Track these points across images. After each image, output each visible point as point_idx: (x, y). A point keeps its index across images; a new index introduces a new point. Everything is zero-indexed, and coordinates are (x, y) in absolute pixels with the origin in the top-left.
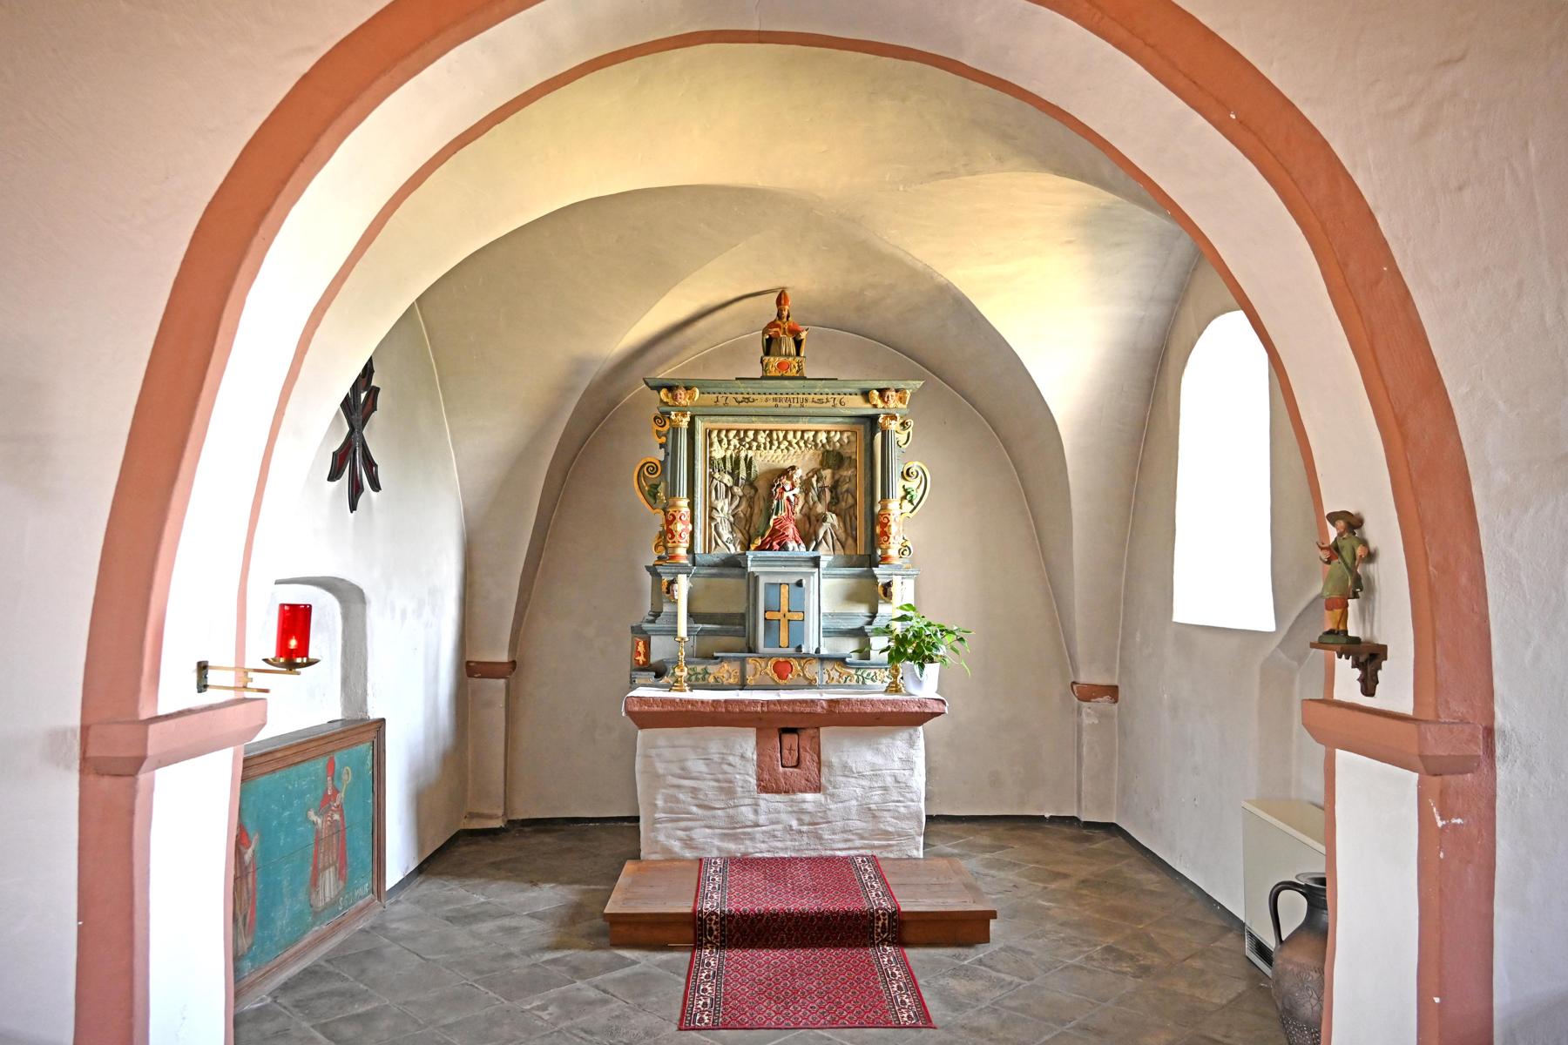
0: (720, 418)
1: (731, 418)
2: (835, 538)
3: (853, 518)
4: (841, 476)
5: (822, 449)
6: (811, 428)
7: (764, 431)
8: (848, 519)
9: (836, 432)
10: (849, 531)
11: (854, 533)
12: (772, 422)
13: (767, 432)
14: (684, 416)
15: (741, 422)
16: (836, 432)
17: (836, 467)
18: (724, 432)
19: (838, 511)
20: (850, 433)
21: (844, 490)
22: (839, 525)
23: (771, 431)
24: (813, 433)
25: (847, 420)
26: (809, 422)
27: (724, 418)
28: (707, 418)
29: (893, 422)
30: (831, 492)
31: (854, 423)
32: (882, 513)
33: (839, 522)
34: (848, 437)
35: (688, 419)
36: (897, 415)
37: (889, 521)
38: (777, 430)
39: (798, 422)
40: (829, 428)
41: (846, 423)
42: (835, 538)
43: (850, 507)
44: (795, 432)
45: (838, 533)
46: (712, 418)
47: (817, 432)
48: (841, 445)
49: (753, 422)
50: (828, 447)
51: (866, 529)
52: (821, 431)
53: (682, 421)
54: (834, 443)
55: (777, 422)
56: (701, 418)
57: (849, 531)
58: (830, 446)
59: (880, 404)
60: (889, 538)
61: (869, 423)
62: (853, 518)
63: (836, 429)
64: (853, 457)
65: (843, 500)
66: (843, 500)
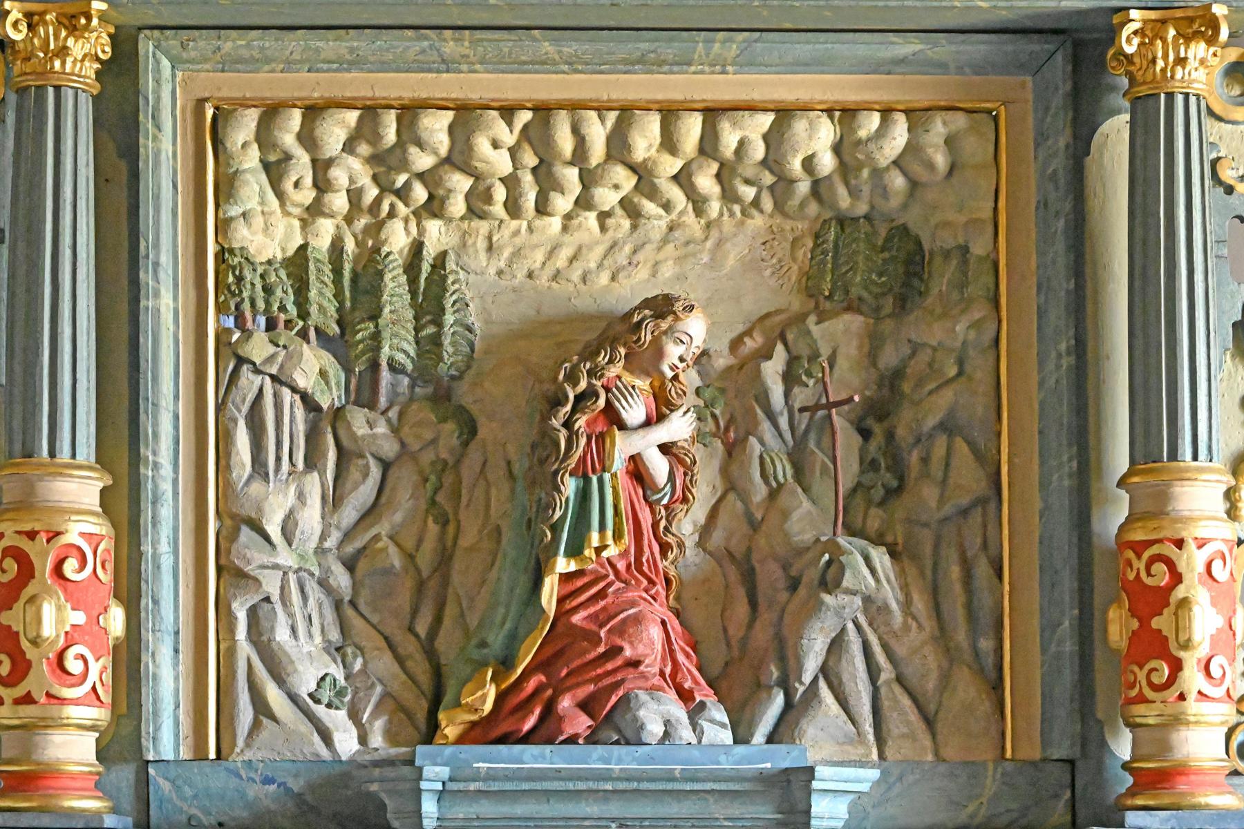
0: (269, 41)
1: (329, 45)
2: (887, 673)
3: (983, 569)
4: (916, 348)
5: (813, 208)
6: (756, 96)
7: (507, 112)
8: (955, 571)
9: (886, 112)
10: (961, 636)
11: (986, 644)
12: (543, 64)
13: (525, 117)
14: (73, 23)
15: (384, 67)
16: (886, 112)
17: (888, 304)
18: (296, 117)
19: (898, 534)
20: (960, 121)
21: (931, 422)
22: (907, 605)
23: (544, 111)
24: (767, 120)
25: (944, 48)
26: (746, 63)
27: (295, 43)
28: (203, 43)
29: (1199, 49)
30: (865, 434)
31: (979, 70)
32: (1139, 536)
33: (905, 588)
34: (950, 142)
35: (97, 42)
36: (1219, 10)
37: (1177, 578)
38: (574, 107)
39: (684, 63)
40: (851, 97)
41: (941, 67)
42: (887, 673)
43: (965, 512)
44: (670, 113)
45: (901, 650)
46: (232, 43)
47: (784, 114)
48: (914, 185)
49: (448, 65)
50: (844, 199)
51: (1050, 627)
52: (806, 108)
53: (63, 52)
54: (877, 173)
55: (574, 64)
56: (172, 40)
57: (961, 636)
58: (854, 193)
60: (1177, 666)
61: (1060, 64)
62: (983, 569)
63: (885, 97)
64: (979, 248)
65: (925, 475)
66: (925, 475)
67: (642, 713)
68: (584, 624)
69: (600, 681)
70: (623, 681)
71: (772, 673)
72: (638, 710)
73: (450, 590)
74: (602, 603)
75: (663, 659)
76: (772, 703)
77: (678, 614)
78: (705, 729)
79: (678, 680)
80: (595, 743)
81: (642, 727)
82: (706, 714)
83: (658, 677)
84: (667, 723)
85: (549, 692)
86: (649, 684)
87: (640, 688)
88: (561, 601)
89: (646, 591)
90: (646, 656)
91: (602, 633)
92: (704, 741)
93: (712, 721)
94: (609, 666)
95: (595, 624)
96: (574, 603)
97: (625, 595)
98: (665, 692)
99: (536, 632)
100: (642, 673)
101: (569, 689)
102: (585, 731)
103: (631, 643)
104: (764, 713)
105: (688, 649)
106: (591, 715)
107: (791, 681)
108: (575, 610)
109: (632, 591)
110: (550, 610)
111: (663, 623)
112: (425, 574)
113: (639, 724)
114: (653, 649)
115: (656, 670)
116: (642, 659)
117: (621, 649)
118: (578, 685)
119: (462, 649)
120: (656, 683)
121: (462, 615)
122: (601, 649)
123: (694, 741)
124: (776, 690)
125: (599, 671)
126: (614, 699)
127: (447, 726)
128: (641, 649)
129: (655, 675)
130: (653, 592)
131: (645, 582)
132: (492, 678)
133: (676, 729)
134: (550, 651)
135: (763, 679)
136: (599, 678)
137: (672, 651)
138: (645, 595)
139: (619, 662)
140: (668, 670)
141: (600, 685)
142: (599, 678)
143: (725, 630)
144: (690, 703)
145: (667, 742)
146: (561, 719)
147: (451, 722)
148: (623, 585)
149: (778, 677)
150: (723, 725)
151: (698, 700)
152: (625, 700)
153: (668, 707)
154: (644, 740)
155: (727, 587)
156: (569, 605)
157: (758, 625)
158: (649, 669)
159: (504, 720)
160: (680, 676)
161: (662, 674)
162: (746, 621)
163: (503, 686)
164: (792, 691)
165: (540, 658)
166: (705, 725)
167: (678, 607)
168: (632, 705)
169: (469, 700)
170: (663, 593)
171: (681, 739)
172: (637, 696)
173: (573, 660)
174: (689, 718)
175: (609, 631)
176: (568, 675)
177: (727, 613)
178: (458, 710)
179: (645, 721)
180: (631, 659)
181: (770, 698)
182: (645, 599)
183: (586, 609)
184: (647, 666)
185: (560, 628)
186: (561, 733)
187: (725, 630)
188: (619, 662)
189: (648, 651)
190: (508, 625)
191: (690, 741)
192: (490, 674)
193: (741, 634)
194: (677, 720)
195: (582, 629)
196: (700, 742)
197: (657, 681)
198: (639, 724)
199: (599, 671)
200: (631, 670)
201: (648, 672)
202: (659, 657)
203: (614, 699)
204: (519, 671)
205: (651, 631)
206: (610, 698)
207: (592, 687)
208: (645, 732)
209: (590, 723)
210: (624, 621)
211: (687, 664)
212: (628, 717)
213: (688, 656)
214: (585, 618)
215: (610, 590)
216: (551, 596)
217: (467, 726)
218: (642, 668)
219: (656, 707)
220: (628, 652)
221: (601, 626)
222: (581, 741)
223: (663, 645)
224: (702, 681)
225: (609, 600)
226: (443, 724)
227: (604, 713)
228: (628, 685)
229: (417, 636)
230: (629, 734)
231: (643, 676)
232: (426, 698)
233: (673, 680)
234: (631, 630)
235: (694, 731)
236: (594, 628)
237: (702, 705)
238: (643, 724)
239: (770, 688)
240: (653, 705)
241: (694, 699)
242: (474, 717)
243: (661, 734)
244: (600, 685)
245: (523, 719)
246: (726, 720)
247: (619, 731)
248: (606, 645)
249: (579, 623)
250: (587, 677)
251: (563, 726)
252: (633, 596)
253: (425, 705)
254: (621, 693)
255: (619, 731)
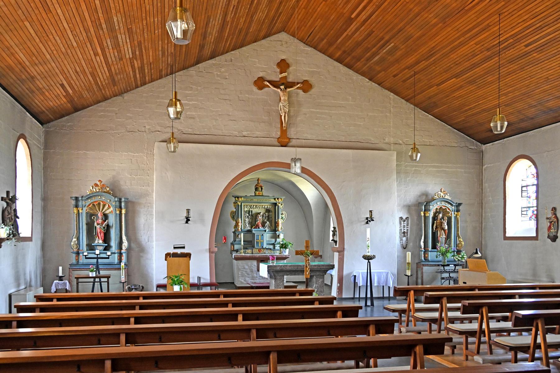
59: (277, 201)
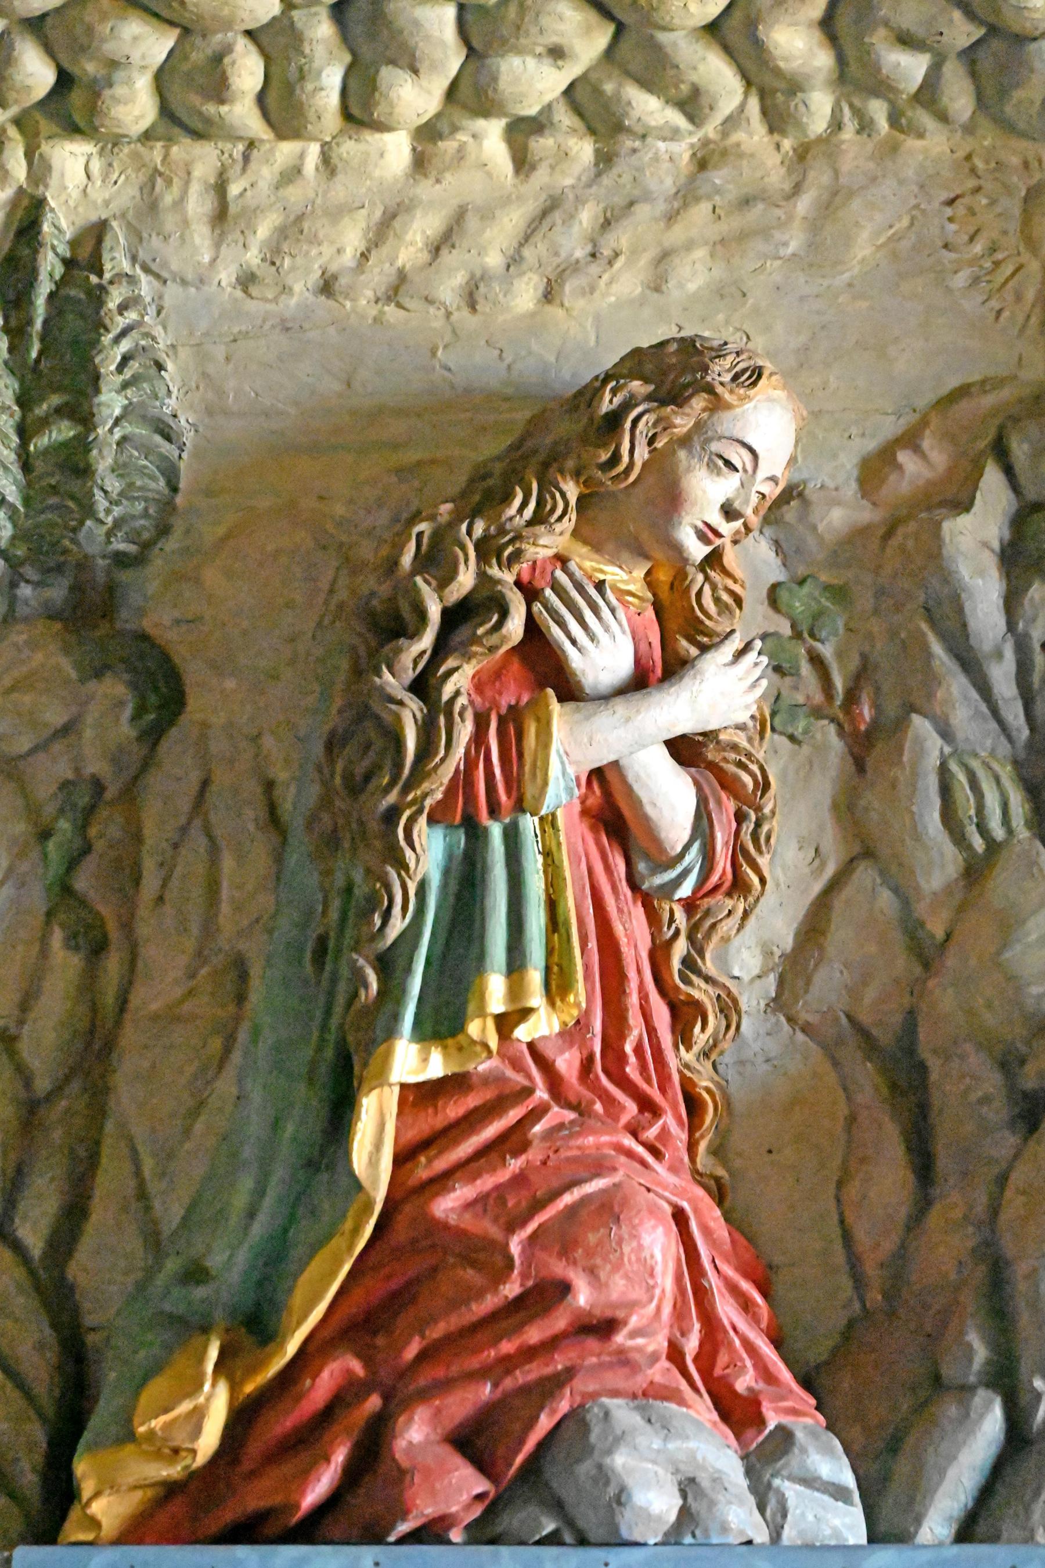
67: (620, 1460)
68: (467, 1222)
69: (508, 1372)
70: (570, 1373)
71: (969, 1352)
72: (609, 1452)
73: (109, 1126)
74: (515, 1165)
75: (679, 1314)
76: (971, 1432)
77: (719, 1193)
78: (791, 1503)
79: (718, 1372)
80: (494, 1541)
81: (621, 1498)
82: (794, 1460)
83: (664, 1363)
84: (688, 1487)
85: (374, 1402)
86: (640, 1382)
87: (615, 1393)
88: (403, 1158)
89: (634, 1132)
90: (632, 1306)
91: (515, 1247)
92: (789, 1535)
93: (810, 1481)
94: (534, 1335)
95: (495, 1220)
96: (442, 1164)
97: (579, 1142)
98: (682, 1402)
99: (337, 1242)
100: (621, 1351)
101: (423, 1396)
102: (468, 1507)
103: (592, 1272)
104: (952, 1458)
105: (746, 1286)
106: (483, 1466)
107: (1023, 1376)
108: (442, 1182)
109: (594, 1132)
110: (375, 1180)
111: (680, 1217)
112: (42, 1085)
113: (612, 1491)
114: (650, 1289)
115: (659, 1343)
116: (620, 1314)
117: (565, 1288)
118: (445, 1386)
119: (141, 1287)
120: (658, 1378)
121: (142, 1194)
122: (511, 1289)
123: (761, 1536)
124: (982, 1394)
125: (507, 1347)
126: (545, 1423)
127: (97, 1494)
128: (618, 1287)
129: (654, 1358)
130: (651, 1133)
131: (631, 1108)
132: (218, 1365)
133: (712, 1504)
134: (375, 1288)
135: (949, 1371)
136: (508, 1364)
137: (702, 1294)
138: (629, 1142)
139: (559, 1322)
140: (692, 1344)
141: (508, 1383)
142: (508, 1364)
143: (847, 1237)
144: (750, 1433)
145: (688, 1540)
146: (401, 1475)
147: (107, 1485)
148: (570, 1115)
149: (988, 1362)
150: (839, 1493)
151: (771, 1426)
152: (576, 1418)
153: (692, 1444)
154: (625, 1534)
155: (852, 1119)
156: (424, 1169)
157: (934, 1218)
158: (640, 1341)
159: (253, 1474)
160: (723, 1359)
161: (675, 1354)
162: (903, 1212)
163: (249, 1388)
164: (1024, 1399)
165: (352, 1307)
166: (792, 1491)
167: (721, 1172)
168: (593, 1438)
169: (156, 1423)
170: (680, 1136)
171: (725, 1529)
172: (607, 1414)
173: (432, 1320)
174: (749, 1472)
175: (533, 1237)
176: (423, 1356)
177: (853, 1190)
178: (130, 1448)
179: (629, 1482)
180: (589, 1313)
181: (966, 1421)
182: (630, 1154)
183: (473, 1179)
184: (634, 1334)
185: (401, 1232)
186: (404, 1515)
187: (847, 1237)
188: (559, 1322)
189: (637, 1293)
190: (258, 1229)
191: (751, 1534)
192: (213, 1353)
193: (889, 1245)
194: (717, 1480)
195: (460, 1234)
196: (776, 1535)
197: (661, 1372)
198: (612, 1491)
199: (507, 1347)
200: (592, 1343)
201: (639, 1349)
202: (667, 1310)
203: (545, 1423)
204: (292, 1347)
205: (646, 1239)
206: (535, 1419)
207: (486, 1391)
208: (628, 1513)
209: (481, 1485)
210: (572, 1211)
211: (742, 1326)
212: (585, 1469)
213: (746, 1305)
214: (469, 1206)
215: (537, 1128)
216: (378, 1146)
217: (150, 1493)
218: (620, 1338)
219: (657, 1444)
220: (583, 1297)
221: (511, 1228)
222: (456, 1535)
223: (678, 1278)
224: (785, 1375)
225: (534, 1155)
226: (87, 1489)
227: (519, 1459)
228: (582, 1384)
229: (17, 1247)
230: (589, 1521)
231: (624, 1360)
232: (41, 1415)
233: (706, 1374)
234: (592, 1238)
235: (761, 1508)
236: (494, 1232)
237: (784, 1437)
238: (622, 1489)
239: (966, 1390)
240: (651, 1441)
241: (761, 1422)
242: (173, 1471)
243: (672, 1517)
244: (508, 1383)
245: (305, 1476)
246: (848, 1479)
247: (558, 1507)
248: (524, 1276)
249: (453, 1219)
250: (474, 1363)
251: (409, 1494)
252: (598, 1147)
253: (38, 1434)
254: (564, 1406)
255: (558, 1507)
